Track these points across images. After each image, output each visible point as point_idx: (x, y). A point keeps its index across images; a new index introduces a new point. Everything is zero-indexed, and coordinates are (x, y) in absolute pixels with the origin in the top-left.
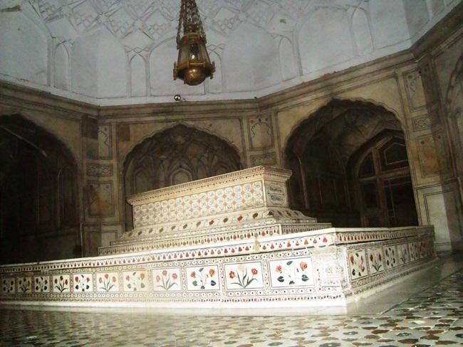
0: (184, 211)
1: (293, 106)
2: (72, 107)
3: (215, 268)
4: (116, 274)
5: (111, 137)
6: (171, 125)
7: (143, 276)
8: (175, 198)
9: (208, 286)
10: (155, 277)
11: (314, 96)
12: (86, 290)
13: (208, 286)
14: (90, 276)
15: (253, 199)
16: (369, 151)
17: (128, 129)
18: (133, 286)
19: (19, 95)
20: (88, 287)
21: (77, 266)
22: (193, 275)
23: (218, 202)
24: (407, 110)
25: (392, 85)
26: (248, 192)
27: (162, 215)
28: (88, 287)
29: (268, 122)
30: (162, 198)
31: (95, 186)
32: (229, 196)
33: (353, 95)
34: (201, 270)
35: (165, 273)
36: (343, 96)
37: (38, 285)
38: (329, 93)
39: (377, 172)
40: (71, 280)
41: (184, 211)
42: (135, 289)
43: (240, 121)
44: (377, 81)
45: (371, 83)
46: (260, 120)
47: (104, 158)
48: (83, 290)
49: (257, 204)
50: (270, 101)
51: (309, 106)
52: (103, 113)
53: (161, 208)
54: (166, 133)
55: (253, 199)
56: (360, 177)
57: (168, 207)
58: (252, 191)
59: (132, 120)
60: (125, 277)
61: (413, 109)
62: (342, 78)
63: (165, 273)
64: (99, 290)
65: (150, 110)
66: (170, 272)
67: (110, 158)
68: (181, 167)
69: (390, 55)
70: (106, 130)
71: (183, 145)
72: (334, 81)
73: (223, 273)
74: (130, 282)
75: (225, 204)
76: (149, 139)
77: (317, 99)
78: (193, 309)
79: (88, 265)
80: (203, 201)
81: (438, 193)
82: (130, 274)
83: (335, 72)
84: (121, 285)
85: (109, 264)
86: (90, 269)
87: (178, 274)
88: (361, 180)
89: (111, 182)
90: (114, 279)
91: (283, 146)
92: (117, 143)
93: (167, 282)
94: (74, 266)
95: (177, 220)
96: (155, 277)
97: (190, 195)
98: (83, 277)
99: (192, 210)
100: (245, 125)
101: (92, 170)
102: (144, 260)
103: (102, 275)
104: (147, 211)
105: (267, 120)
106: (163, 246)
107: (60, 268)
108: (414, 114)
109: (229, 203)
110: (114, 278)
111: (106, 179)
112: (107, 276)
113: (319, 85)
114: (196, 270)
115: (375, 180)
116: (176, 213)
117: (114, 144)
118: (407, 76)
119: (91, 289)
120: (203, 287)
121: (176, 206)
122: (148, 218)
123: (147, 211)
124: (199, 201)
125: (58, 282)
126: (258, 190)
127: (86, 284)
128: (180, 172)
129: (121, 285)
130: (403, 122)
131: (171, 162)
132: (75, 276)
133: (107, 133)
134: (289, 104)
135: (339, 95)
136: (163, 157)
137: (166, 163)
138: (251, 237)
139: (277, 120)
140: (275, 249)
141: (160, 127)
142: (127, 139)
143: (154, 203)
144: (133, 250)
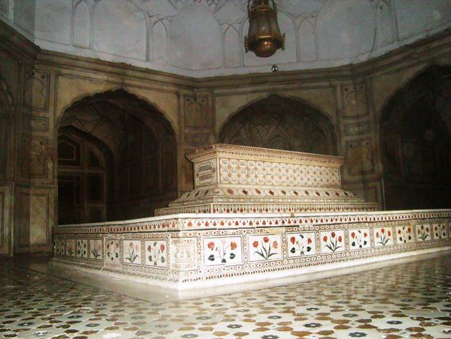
0: (280, 178)
1: (78, 77)
4: (390, 229)
7: (409, 230)
8: (272, 162)
9: (443, 237)
10: (375, 234)
11: (105, 78)
12: (364, 246)
14: (367, 231)
15: (334, 181)
18: (403, 239)
20: (365, 243)
21: (352, 221)
23: (310, 177)
24: (183, 125)
25: (175, 100)
27: (256, 177)
28: (365, 243)
29: (45, 80)
30: (258, 158)
32: (318, 173)
33: (142, 94)
36: (131, 90)
37: (295, 246)
38: (121, 81)
40: (346, 236)
41: (280, 178)
42: (405, 241)
43: (20, 66)
44: (163, 91)
45: (158, 90)
48: (361, 246)
49: (336, 185)
50: (56, 59)
51: (97, 84)
53: (256, 169)
55: (334, 181)
57: (264, 169)
58: (333, 174)
60: (397, 231)
61: (187, 126)
62: (138, 74)
63: (422, 227)
64: (377, 245)
69: (183, 76)
72: (130, 73)
74: (401, 235)
75: (315, 180)
77: (108, 81)
78: (267, 280)
79: (364, 220)
80: (298, 172)
82: (401, 228)
83: (131, 65)
84: (395, 239)
85: (376, 220)
86: (367, 224)
87: (429, 228)
90: (389, 234)
91: (58, 116)
94: (348, 221)
95: (273, 185)
96: (417, 231)
97: (287, 164)
98: (360, 232)
99: (288, 178)
100: (23, 72)
102: (264, 223)
103: (378, 230)
104: (238, 168)
105: (43, 77)
106: (301, 210)
107: (329, 222)
108: (187, 131)
109: (318, 179)
110: (389, 233)
112: (383, 231)
113: (115, 70)
116: (272, 177)
118: (186, 98)
119: (368, 245)
121: (272, 170)
122: (239, 176)
123: (238, 168)
124: (294, 171)
125: (328, 240)
127: (364, 239)
129: (395, 239)
130: (177, 132)
132: (350, 232)
134: (75, 73)
135: (128, 87)
138: (257, 211)
139: (56, 82)
140: (266, 225)
143: (247, 160)
144: (267, 210)
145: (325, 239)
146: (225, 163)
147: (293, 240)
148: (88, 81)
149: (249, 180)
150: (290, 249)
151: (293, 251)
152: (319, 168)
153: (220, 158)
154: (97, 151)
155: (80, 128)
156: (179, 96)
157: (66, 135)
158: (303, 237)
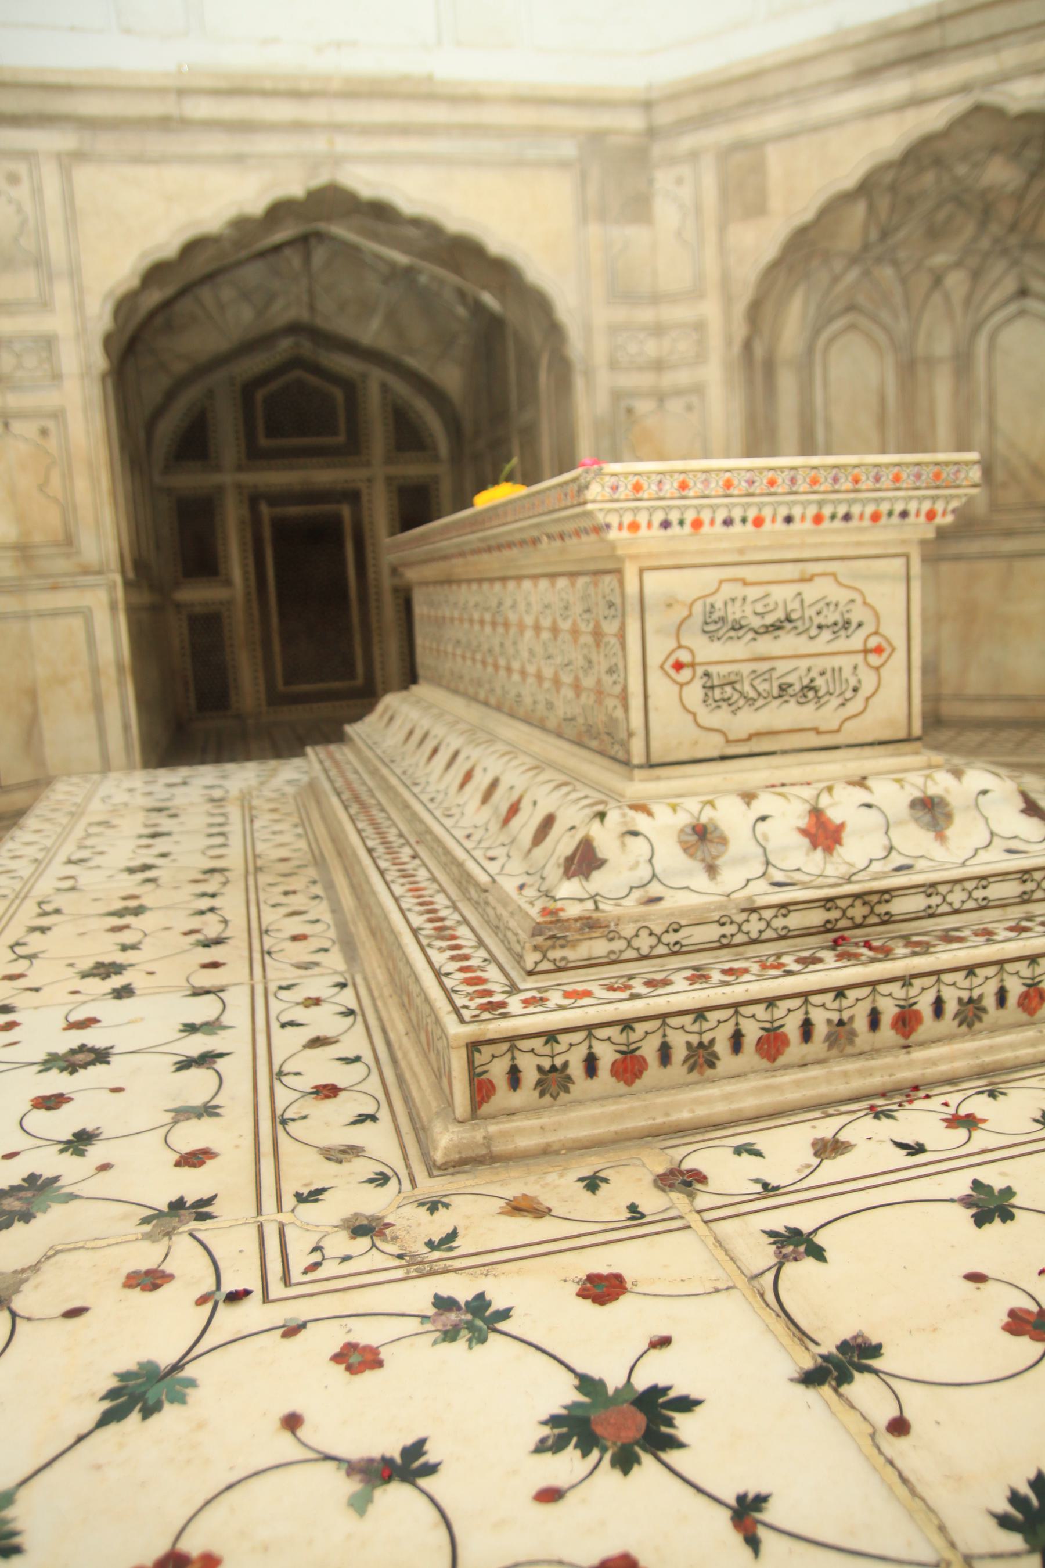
2: (529, 116)
5: (698, 210)
6: (934, 118)
17: (759, 168)
19: (316, 112)
31: (644, 407)
47: (673, 298)
52: (664, 116)
54: (921, 154)
59: (773, 121)
65: (842, 66)
67: (696, 293)
68: (1023, 292)
70: (679, 181)
71: (1019, 196)
76: (846, 198)
89: (698, 389)
92: (722, 229)
101: (633, 348)
111: (682, 377)
117: (711, 235)
128: (1022, 313)
131: (976, 275)
133: (686, 192)
136: (940, 259)
137: (956, 282)
141: (889, 138)
142: (757, 209)
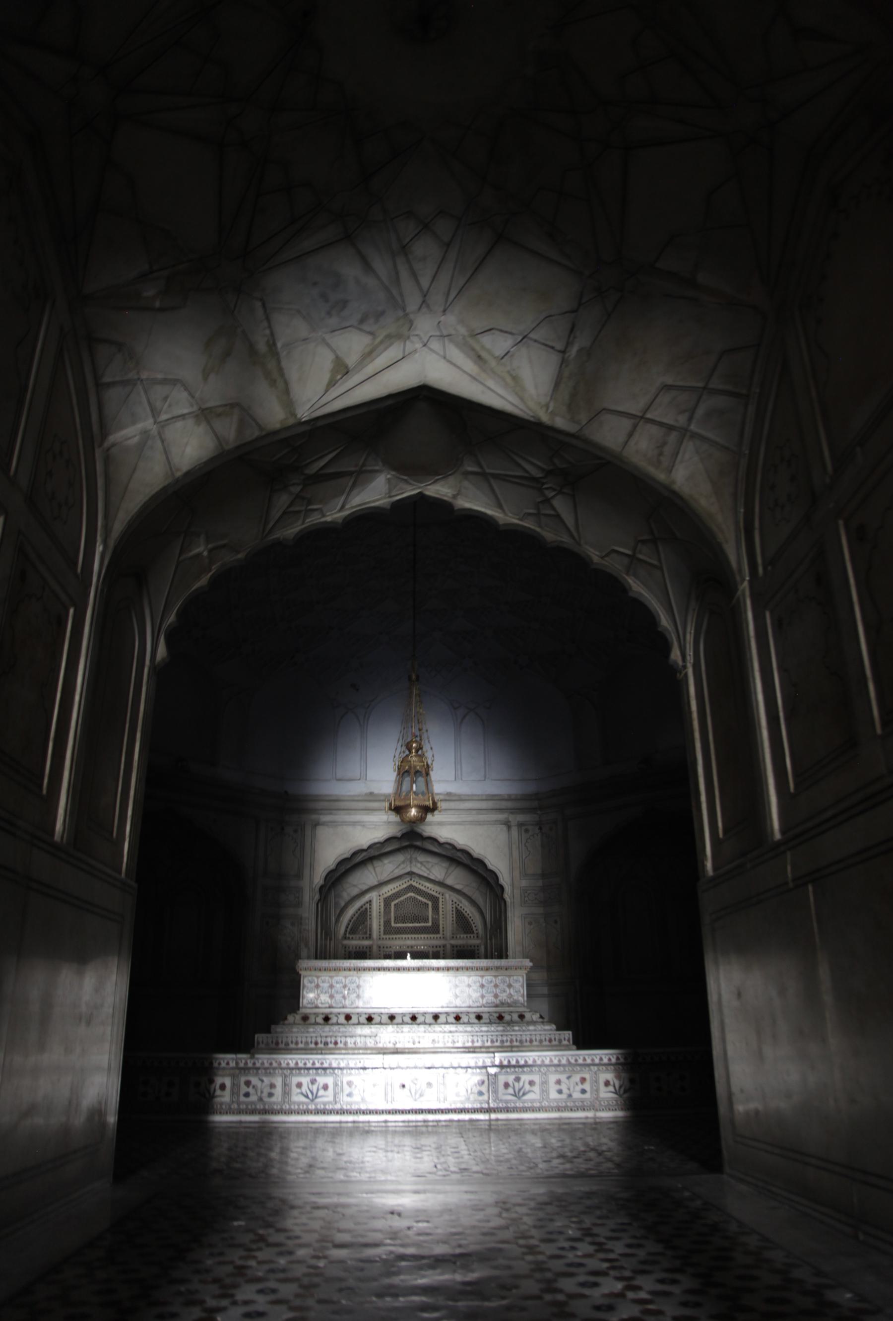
3: (587, 1076)
9: (577, 1095)
13: (577, 1095)
16: (367, 898)
22: (559, 1082)
26: (502, 986)
34: (568, 1078)
35: (518, 1079)
39: (375, 935)
46: (283, 829)
56: (345, 938)
58: (510, 986)
66: (525, 1078)
69: (509, 795)
73: (597, 1081)
81: (543, 996)
88: (346, 942)
93: (520, 1090)
114: (563, 1077)
115: (370, 947)
118: (523, 828)
120: (570, 1096)
123: (331, 986)
126: (517, 985)
145: (299, 1085)
146: (311, 982)
147: (248, 1083)
148: (359, 828)
149: (347, 1003)
150: (243, 1092)
151: (247, 1095)
152: (480, 979)
153: (305, 977)
154: (468, 909)
155: (426, 875)
156: (509, 827)
157: (414, 884)
158: (262, 1081)
